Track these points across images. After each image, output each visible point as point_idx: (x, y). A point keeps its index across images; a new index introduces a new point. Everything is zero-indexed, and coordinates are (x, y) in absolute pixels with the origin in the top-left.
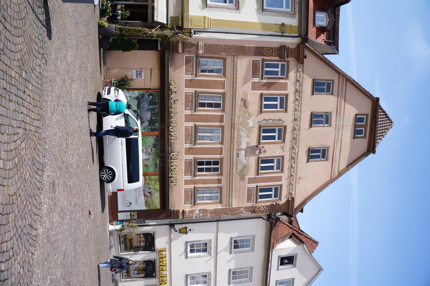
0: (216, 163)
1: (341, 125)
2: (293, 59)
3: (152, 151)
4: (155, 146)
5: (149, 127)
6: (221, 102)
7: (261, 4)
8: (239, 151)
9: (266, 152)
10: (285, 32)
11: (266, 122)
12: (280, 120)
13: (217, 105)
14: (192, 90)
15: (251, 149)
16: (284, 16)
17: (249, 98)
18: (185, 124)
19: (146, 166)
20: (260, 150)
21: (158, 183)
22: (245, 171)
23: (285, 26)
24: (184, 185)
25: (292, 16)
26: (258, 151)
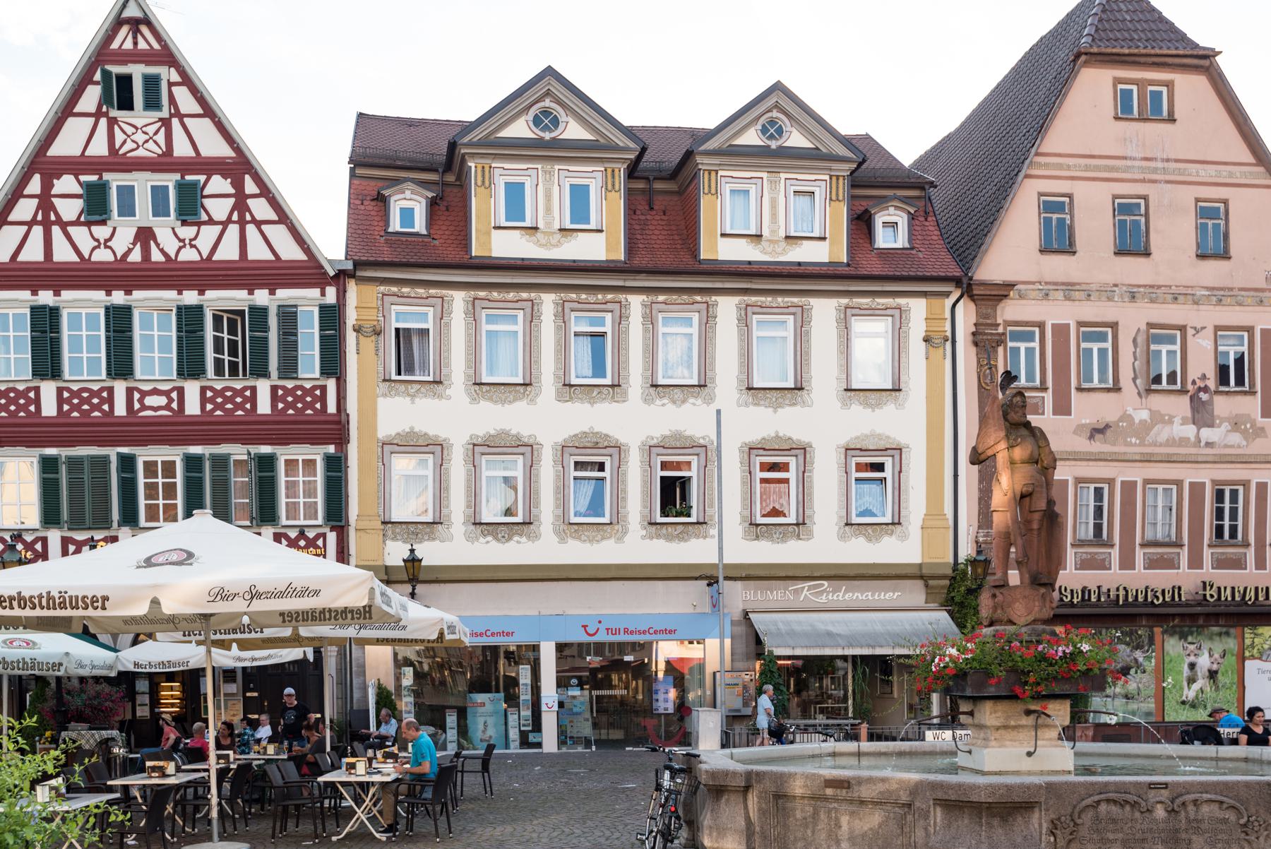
0: (1219, 496)
1: (1145, 164)
2: (999, 312)
3: (1195, 641)
4: (1183, 636)
5: (1146, 648)
6: (1092, 486)
7: (884, 393)
8: (1200, 441)
9: (1205, 375)
10: (943, 334)
11: (1139, 376)
12: (1135, 341)
13: (1098, 493)
14: (1071, 555)
15: (1198, 412)
16: (907, 337)
17: (1088, 421)
18: (1140, 570)
19: (1224, 655)
20: (1200, 389)
21: (1261, 630)
22: (1246, 426)
23: (928, 333)
24: (1266, 569)
25: (904, 316)
26: (1202, 395)
